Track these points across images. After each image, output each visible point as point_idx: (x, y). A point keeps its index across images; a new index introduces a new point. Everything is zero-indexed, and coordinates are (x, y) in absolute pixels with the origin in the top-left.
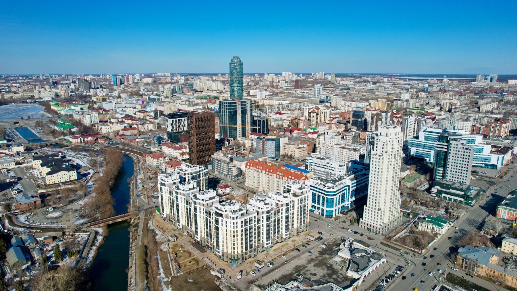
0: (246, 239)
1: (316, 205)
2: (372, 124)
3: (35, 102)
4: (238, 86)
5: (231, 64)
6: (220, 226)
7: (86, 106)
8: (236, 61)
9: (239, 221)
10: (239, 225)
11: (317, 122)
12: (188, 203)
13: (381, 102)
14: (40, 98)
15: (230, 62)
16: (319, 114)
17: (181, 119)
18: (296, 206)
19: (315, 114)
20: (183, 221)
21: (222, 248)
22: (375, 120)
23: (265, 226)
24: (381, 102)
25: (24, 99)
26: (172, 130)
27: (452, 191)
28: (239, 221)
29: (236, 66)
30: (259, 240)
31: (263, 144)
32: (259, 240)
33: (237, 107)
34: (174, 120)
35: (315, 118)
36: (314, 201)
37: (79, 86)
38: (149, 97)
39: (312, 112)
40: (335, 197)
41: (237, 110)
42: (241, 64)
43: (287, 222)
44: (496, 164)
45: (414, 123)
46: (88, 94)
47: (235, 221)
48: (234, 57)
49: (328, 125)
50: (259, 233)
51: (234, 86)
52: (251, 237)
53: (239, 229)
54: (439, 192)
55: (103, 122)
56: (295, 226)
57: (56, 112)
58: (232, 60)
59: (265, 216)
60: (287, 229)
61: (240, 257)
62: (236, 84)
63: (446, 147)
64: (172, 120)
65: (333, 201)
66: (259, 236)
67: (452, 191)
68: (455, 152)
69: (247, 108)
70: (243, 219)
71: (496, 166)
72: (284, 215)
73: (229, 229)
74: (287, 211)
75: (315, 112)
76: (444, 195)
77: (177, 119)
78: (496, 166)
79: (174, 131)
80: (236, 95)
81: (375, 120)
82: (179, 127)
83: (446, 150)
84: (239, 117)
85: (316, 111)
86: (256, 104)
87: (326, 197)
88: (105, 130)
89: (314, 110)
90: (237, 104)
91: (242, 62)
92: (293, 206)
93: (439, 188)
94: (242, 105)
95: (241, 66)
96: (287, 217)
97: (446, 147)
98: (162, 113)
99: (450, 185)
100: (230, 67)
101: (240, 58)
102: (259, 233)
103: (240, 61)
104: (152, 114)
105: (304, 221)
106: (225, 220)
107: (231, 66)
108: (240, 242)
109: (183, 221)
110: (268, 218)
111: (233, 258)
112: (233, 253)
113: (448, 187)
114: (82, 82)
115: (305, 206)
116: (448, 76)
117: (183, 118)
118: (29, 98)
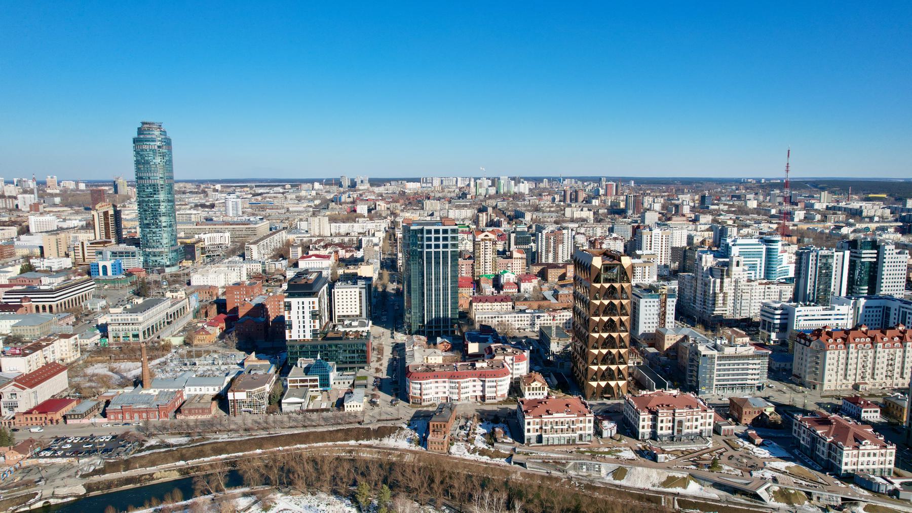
2: (547, 252)
5: (135, 141)
15: (135, 135)
19: (489, 244)
29: (159, 147)
31: (663, 305)
39: (482, 240)
45: (660, 237)
48: (143, 123)
51: (159, 201)
58: (140, 131)
62: (162, 196)
63: (875, 255)
75: (490, 240)
80: (164, 224)
81: (552, 245)
89: (487, 236)
91: (168, 135)
97: (875, 255)
101: (164, 128)
116: (320, 181)
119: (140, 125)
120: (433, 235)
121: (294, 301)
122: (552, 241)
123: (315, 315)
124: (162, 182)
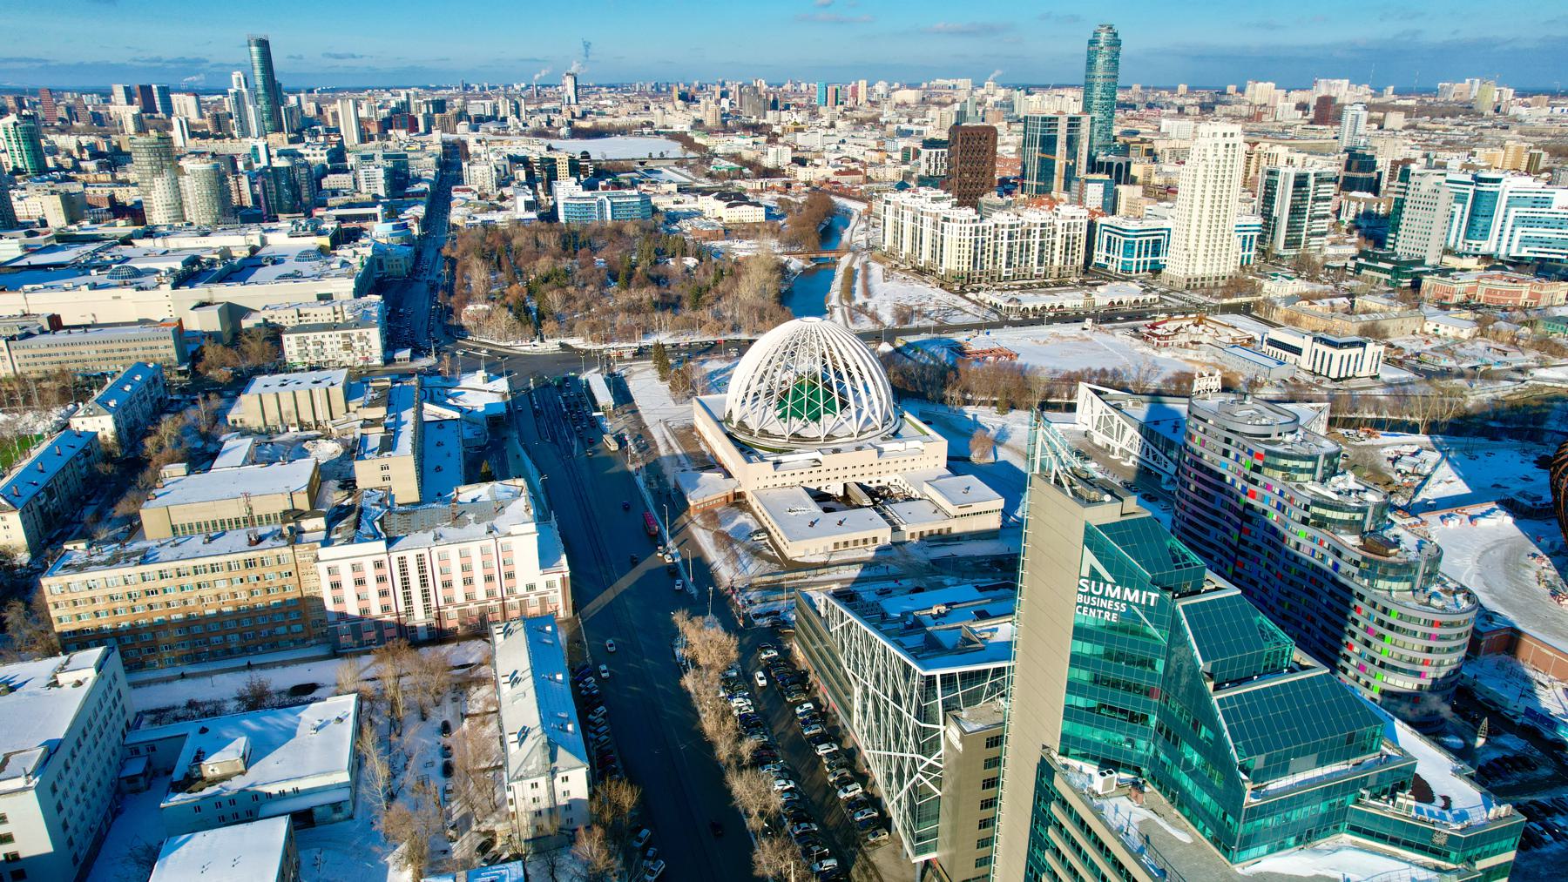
0: (975, 254)
1: (1111, 255)
3: (657, 133)
4: (1101, 98)
6: (945, 234)
7: (763, 139)
8: (1103, 35)
9: (968, 226)
10: (968, 232)
11: (1247, 173)
12: (914, 219)
13: (1511, 151)
14: (665, 127)
16: (1255, 156)
18: (1059, 233)
20: (907, 248)
21: (946, 265)
23: (1005, 245)
24: (1511, 151)
25: (636, 127)
27: (1381, 265)
28: (968, 226)
30: (995, 263)
32: (995, 263)
33: (1059, 128)
34: (934, 151)
36: (1108, 250)
37: (741, 104)
40: (1137, 240)
41: (1059, 134)
42: (1115, 43)
43: (1041, 251)
46: (761, 121)
47: (963, 225)
50: (995, 252)
52: (983, 253)
53: (967, 237)
55: (801, 162)
56: (1056, 263)
57: (705, 148)
58: (1096, 34)
59: (1006, 231)
60: (1040, 262)
61: (965, 276)
65: (1133, 248)
66: (995, 258)
67: (1381, 265)
69: (1082, 131)
70: (974, 225)
72: (1037, 240)
74: (1042, 236)
79: (932, 173)
84: (1061, 147)
86: (1146, 146)
87: (1123, 239)
92: (1054, 233)
94: (1069, 125)
95: (1114, 49)
96: (1041, 244)
102: (995, 252)
103: (1116, 35)
104: (898, 156)
105: (1072, 260)
106: (951, 224)
108: (966, 255)
109: (907, 248)
110: (1010, 236)
115: (1074, 238)
118: (643, 126)
123: (928, 160)
124: (1098, 81)
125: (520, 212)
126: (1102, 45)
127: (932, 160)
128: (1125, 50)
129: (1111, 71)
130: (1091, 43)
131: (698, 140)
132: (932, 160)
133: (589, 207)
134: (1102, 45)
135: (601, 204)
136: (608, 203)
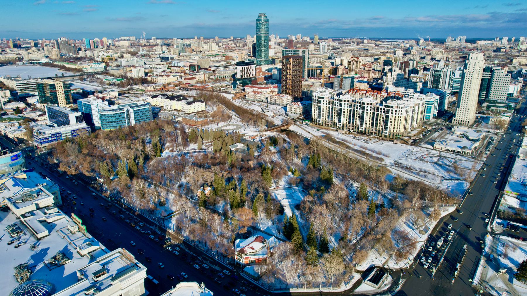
4: (265, 42)
5: (257, 20)
8: (263, 17)
17: (247, 66)
19: (355, 63)
20: (344, 119)
22: (403, 68)
26: (241, 76)
27: (497, 105)
31: (341, 81)
34: (244, 67)
35: (355, 66)
38: (159, 56)
39: (352, 61)
42: (267, 21)
44: (512, 93)
49: (367, 72)
54: (488, 107)
58: (259, 17)
63: (490, 76)
64: (242, 67)
67: (497, 105)
68: (498, 78)
69: (306, 56)
71: (513, 94)
73: (397, 115)
75: (355, 61)
76: (492, 108)
77: (245, 66)
78: (513, 94)
81: (403, 68)
82: (247, 73)
83: (490, 78)
85: (356, 59)
88: (163, 80)
90: (300, 53)
93: (488, 104)
97: (490, 76)
98: (199, 68)
99: (497, 101)
100: (257, 24)
101: (266, 15)
107: (259, 23)
111: (398, 135)
112: (398, 131)
113: (495, 102)
114: (64, 44)
117: (249, 66)
119: (259, 15)
120: (288, 52)
121: (237, 67)
122: (403, 66)
123: (241, 71)
124: (263, 35)
125: (74, 125)
126: (263, 21)
127: (243, 71)
128: (270, 22)
129: (266, 31)
130: (257, 20)
131: (68, 66)
132: (243, 71)
133: (120, 115)
134: (263, 21)
135: (128, 112)
136: (132, 111)
